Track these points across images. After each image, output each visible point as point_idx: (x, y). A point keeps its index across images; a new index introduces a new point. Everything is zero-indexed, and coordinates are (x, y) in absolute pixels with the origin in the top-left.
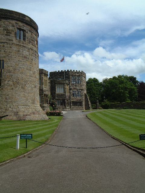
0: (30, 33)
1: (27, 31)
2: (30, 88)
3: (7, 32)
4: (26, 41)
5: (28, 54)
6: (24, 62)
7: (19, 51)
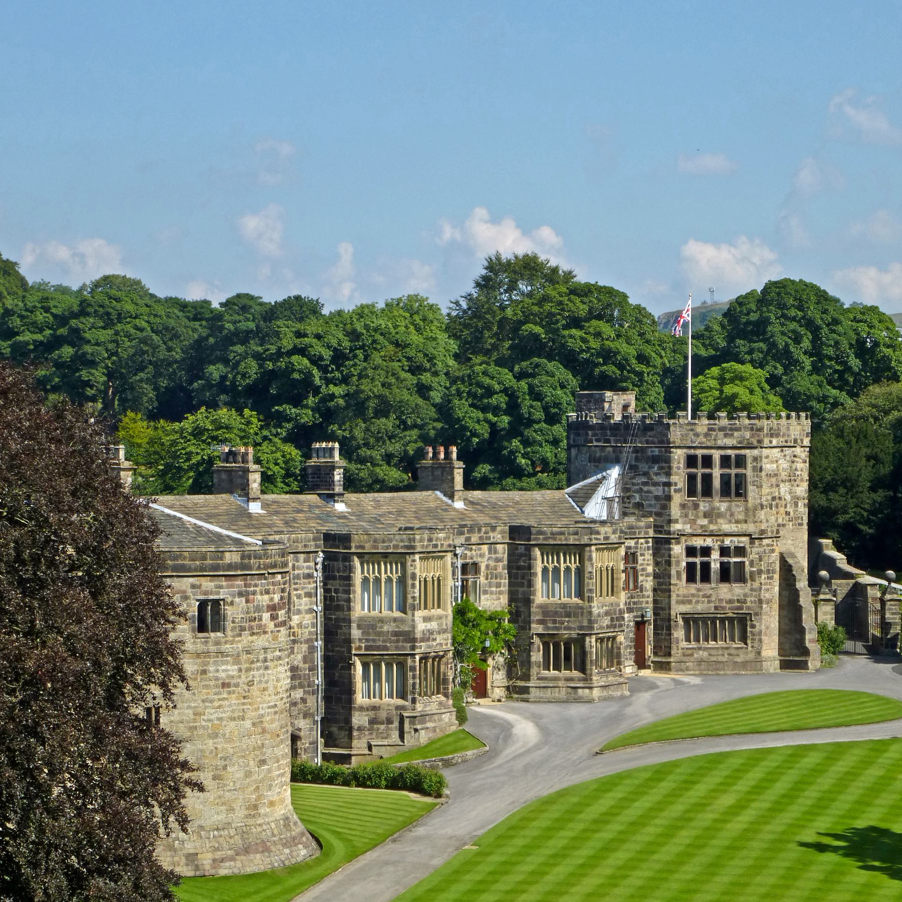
0: (243, 599)
1: (229, 600)
2: (240, 775)
4: (229, 633)
5: (235, 673)
6: (219, 700)
7: (204, 672)
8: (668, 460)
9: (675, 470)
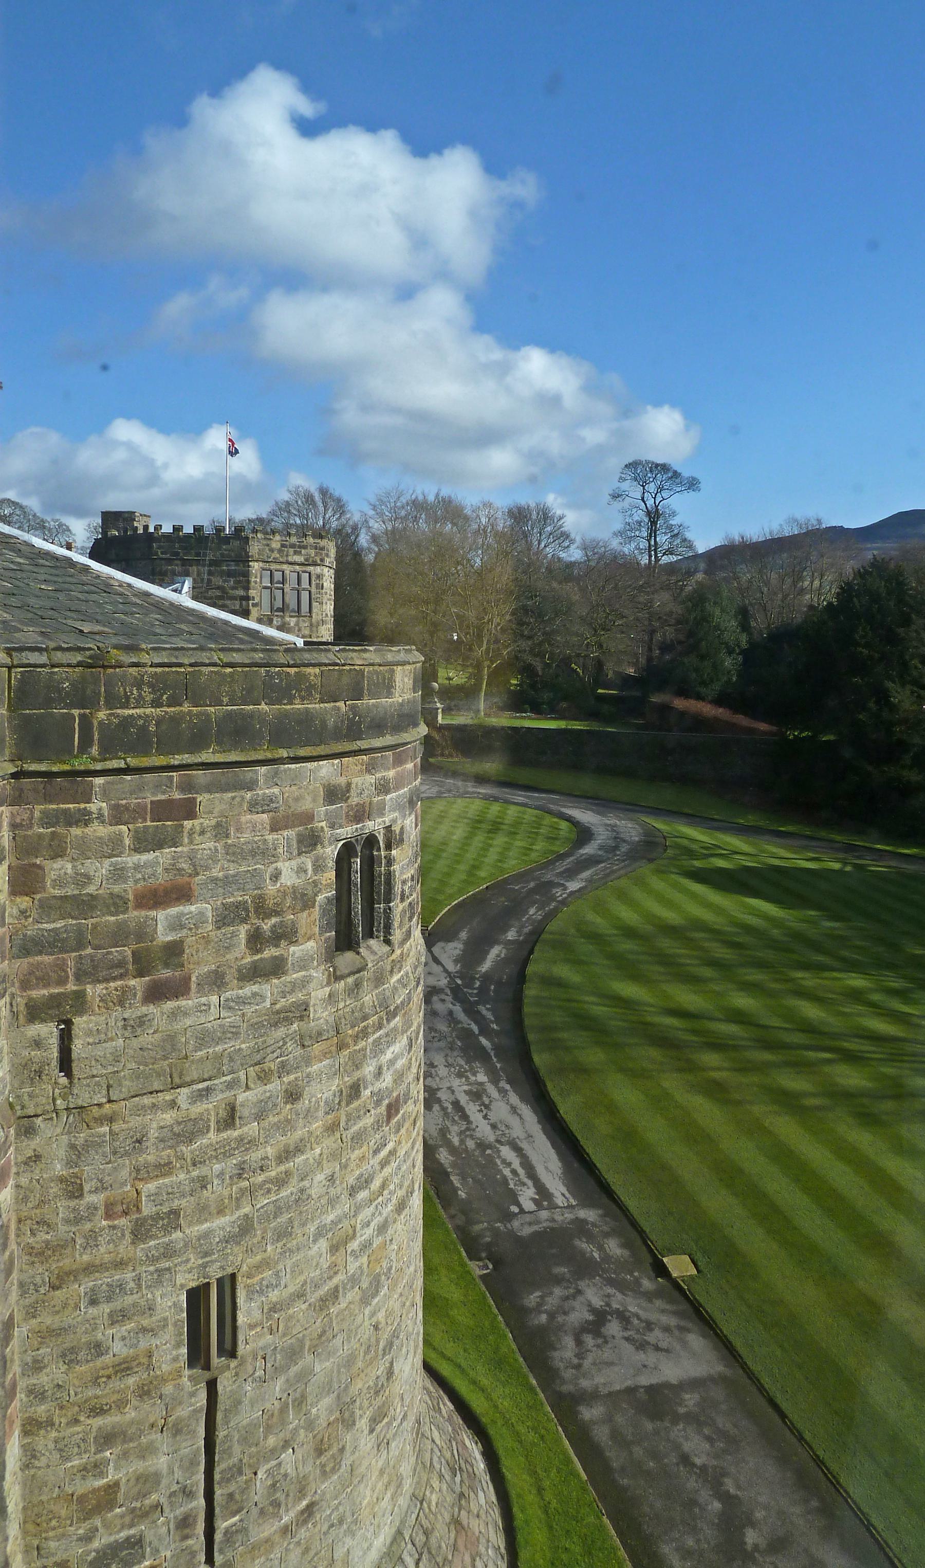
3: (256, 940)
8: (246, 575)
9: (253, 584)
